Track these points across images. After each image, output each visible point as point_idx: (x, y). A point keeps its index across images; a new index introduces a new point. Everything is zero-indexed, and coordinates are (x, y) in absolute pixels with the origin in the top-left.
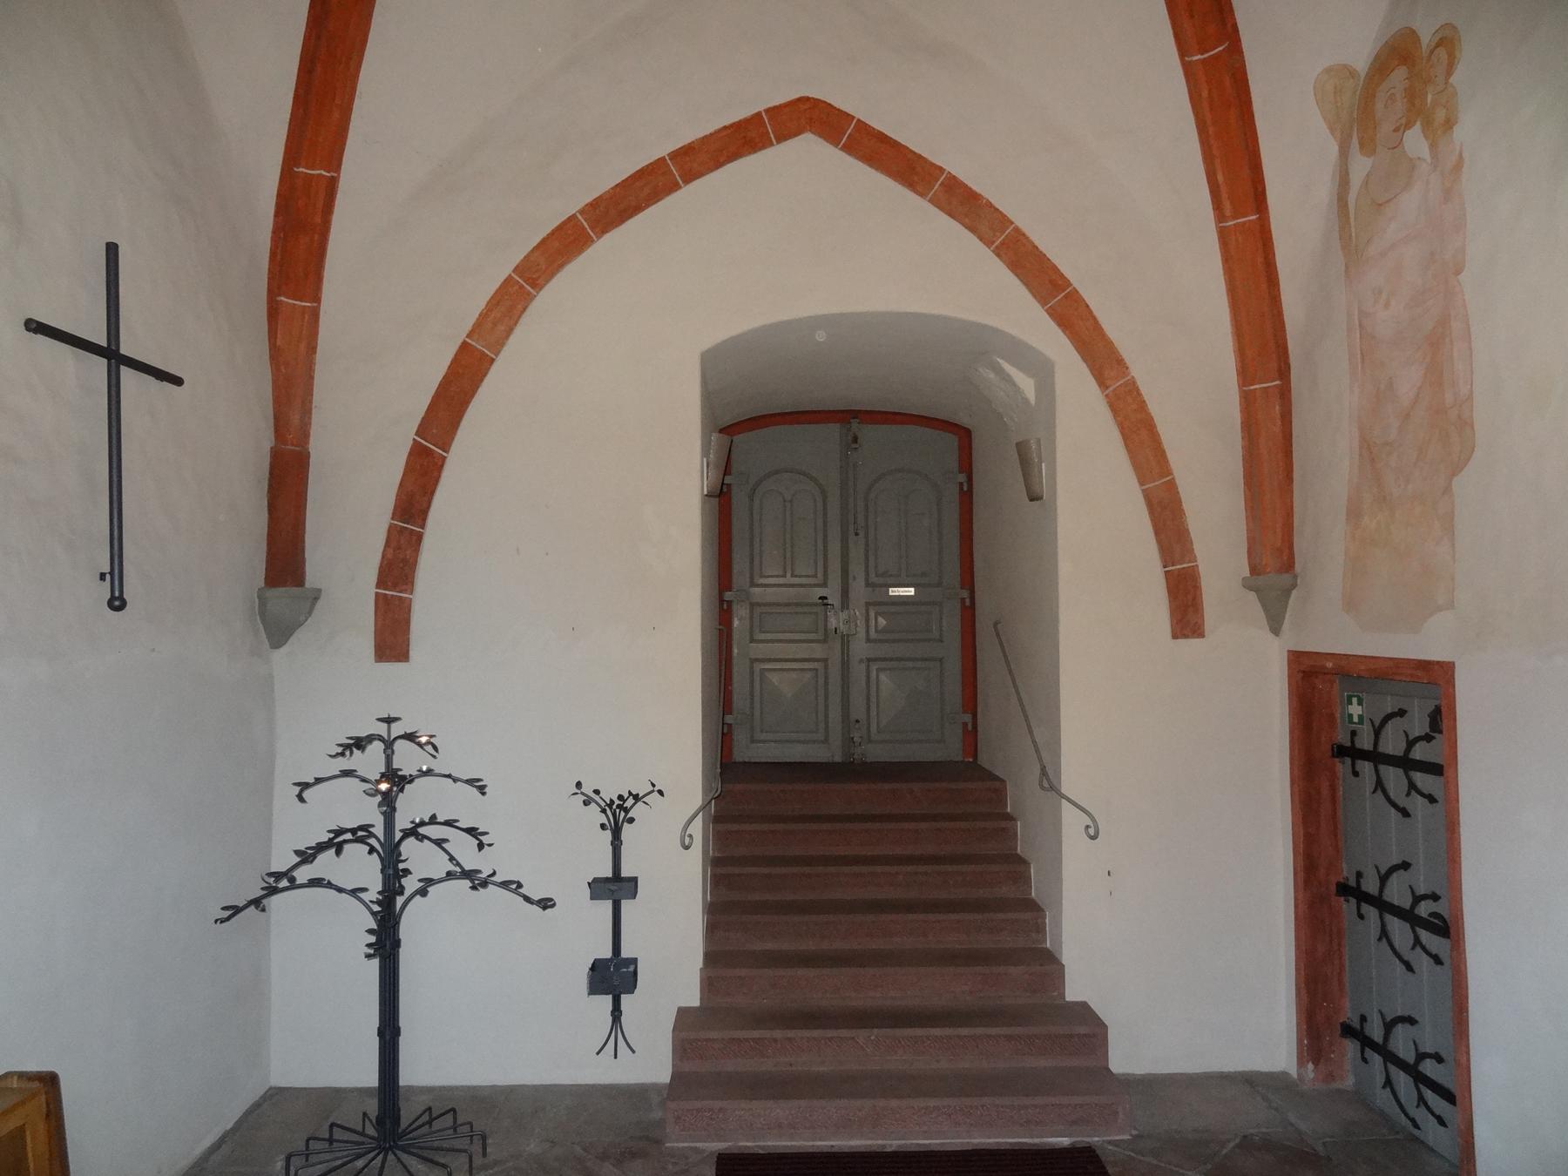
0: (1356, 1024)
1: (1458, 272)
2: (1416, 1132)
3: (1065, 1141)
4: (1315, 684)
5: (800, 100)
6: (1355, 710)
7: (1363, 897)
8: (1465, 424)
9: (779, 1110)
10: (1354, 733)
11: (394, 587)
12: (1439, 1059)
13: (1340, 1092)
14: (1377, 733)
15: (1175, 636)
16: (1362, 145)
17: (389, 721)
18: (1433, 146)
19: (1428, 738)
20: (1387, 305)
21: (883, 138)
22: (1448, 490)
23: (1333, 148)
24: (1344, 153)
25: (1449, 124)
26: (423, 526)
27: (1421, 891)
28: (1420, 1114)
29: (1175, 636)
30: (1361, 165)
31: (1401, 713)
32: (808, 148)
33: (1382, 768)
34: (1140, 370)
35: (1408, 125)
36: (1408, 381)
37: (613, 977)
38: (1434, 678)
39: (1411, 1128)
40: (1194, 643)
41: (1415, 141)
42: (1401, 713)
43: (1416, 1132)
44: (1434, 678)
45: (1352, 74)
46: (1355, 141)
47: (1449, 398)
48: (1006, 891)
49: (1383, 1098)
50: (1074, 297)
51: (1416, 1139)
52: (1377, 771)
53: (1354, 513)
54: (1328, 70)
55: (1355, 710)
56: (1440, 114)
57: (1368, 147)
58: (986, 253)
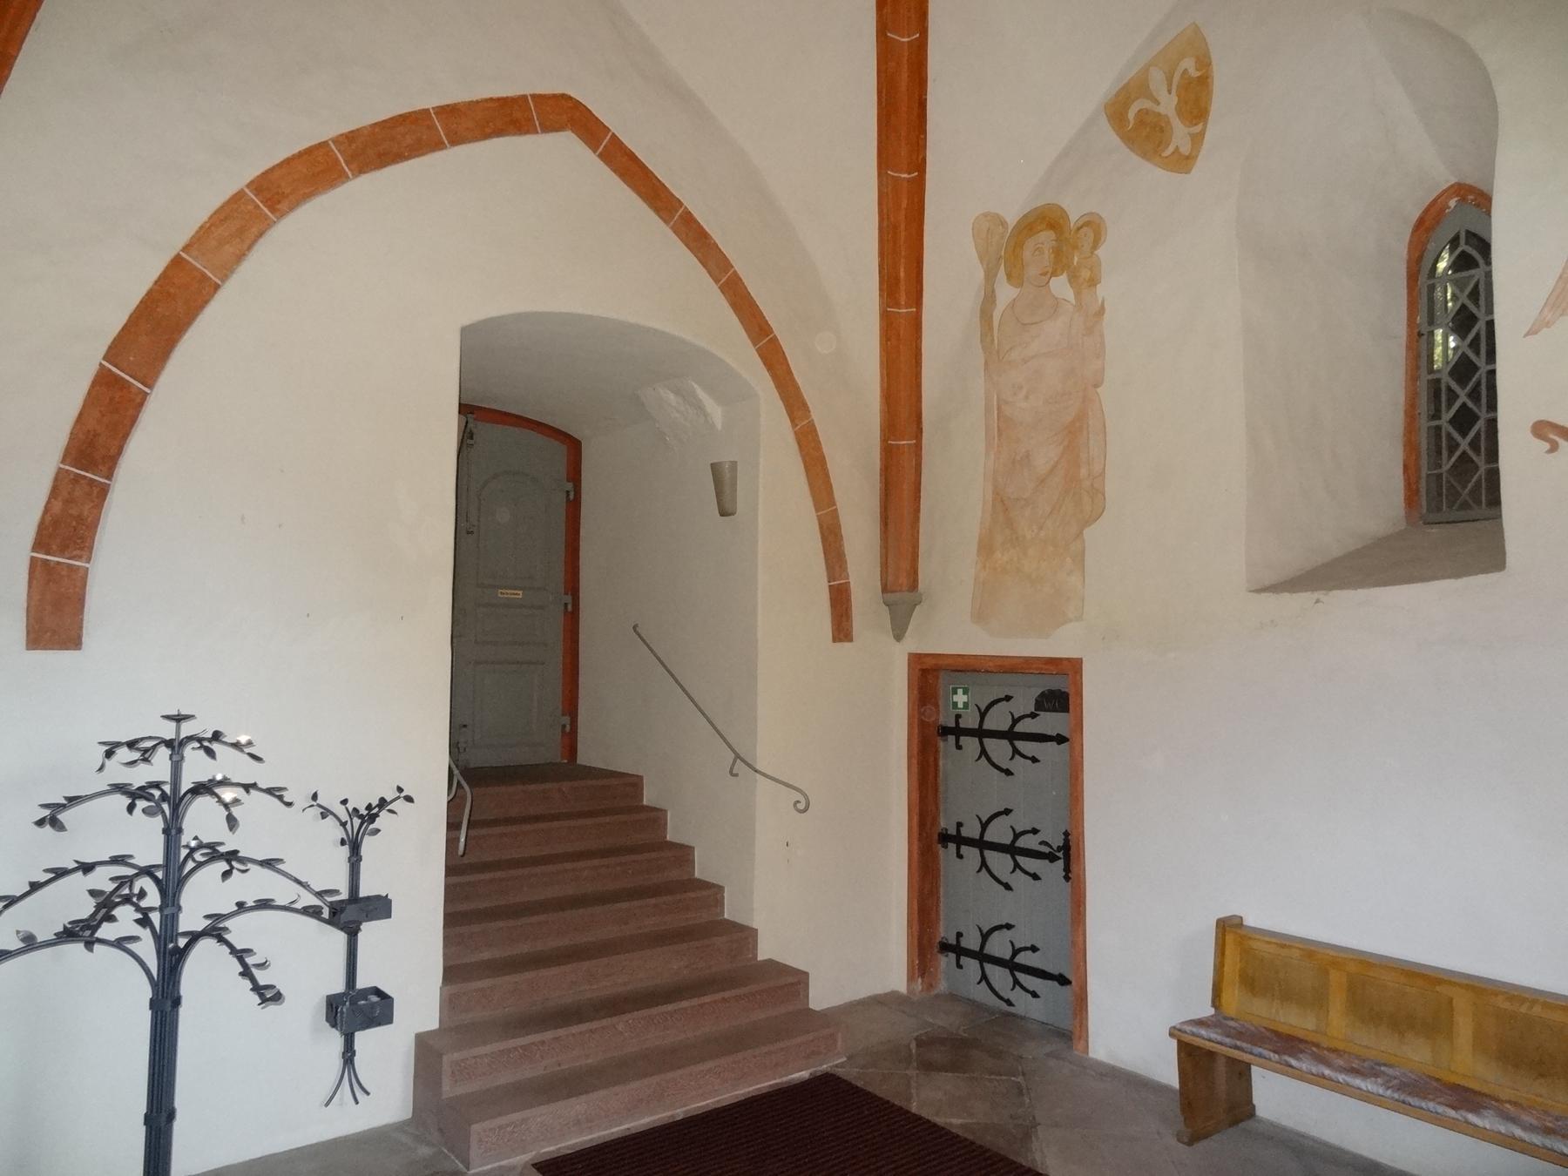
0: (952, 941)
1: (1096, 386)
2: (1011, 1009)
3: (804, 1075)
4: (929, 677)
5: (563, 96)
6: (960, 698)
7: (960, 840)
8: (1097, 493)
9: (577, 1106)
10: (958, 717)
11: (62, 551)
12: (1034, 949)
13: (937, 996)
14: (983, 715)
15: (834, 640)
16: (1009, 276)
17: (179, 719)
18: (1078, 294)
19: (1033, 716)
20: (1027, 397)
21: (632, 157)
22: (1080, 534)
24: (990, 277)
25: (1093, 282)
26: (109, 476)
27: (1019, 829)
28: (1017, 996)
29: (834, 640)
30: (1006, 293)
31: (1008, 698)
32: (565, 145)
34: (818, 415)
35: (1054, 274)
36: (1045, 456)
37: (357, 1009)
38: (1072, 667)
39: (1004, 1006)
40: (847, 644)
41: (1060, 286)
42: (1008, 698)
43: (1011, 1009)
44: (1072, 667)
45: (1003, 223)
46: (1002, 273)
47: (1083, 472)
48: (674, 874)
49: (981, 994)
51: (1014, 1015)
52: (981, 743)
53: (986, 548)
54: (985, 215)
55: (960, 698)
56: (1085, 274)
57: (1015, 277)
58: (715, 288)
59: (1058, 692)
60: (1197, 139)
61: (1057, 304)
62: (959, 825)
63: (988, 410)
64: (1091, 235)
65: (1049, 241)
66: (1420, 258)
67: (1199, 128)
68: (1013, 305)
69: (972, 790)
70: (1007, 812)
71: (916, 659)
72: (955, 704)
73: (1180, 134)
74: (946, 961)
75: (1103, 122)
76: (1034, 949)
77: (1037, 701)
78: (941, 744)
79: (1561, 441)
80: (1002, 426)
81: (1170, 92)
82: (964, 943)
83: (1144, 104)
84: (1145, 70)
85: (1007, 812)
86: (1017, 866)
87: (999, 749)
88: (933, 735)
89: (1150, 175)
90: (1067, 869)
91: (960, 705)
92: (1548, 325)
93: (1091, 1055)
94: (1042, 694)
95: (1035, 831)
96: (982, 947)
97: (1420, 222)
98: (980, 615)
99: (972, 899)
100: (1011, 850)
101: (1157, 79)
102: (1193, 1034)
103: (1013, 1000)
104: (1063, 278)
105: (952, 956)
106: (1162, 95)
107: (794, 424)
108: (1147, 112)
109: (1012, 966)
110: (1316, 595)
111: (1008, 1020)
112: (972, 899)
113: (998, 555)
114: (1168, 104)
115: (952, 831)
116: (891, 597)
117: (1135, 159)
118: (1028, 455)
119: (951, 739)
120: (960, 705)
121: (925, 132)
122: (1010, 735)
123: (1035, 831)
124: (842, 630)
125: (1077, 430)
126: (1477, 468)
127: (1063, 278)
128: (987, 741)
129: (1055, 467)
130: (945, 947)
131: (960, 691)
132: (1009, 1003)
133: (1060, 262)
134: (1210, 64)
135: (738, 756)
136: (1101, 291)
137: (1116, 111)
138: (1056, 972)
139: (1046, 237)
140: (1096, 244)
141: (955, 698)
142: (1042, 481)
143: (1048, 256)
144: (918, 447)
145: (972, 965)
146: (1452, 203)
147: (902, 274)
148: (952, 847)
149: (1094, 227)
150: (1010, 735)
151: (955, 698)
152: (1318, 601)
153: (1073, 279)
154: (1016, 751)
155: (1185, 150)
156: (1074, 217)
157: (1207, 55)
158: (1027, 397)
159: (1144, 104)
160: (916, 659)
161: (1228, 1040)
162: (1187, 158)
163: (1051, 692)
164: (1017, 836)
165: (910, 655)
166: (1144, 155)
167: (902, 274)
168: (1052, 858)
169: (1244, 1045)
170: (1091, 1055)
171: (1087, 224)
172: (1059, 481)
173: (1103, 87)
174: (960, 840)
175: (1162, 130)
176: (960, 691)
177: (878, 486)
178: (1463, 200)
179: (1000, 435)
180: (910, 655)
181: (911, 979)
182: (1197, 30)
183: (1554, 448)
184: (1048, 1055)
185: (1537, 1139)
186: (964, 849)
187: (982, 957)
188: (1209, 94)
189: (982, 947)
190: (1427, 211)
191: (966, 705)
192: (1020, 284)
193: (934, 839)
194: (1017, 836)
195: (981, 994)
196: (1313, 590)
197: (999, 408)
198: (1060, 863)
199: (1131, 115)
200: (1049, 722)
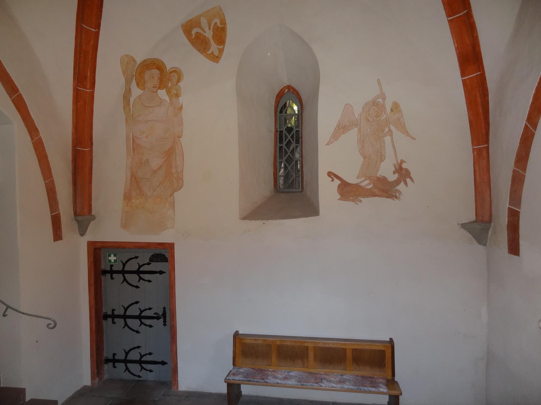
0: (111, 357)
1: (179, 137)
4: (97, 251)
6: (112, 258)
8: (180, 179)
10: (112, 266)
12: (150, 354)
14: (124, 265)
16: (138, 85)
18: (170, 99)
19: (148, 264)
20: (147, 137)
22: (172, 195)
23: (123, 80)
24: (128, 82)
25: (177, 95)
28: (143, 374)
30: (136, 91)
31: (136, 257)
33: (126, 275)
35: (159, 88)
36: (156, 162)
38: (171, 246)
39: (136, 378)
40: (60, 242)
41: (162, 94)
42: (136, 257)
44: (171, 246)
45: (134, 61)
46: (134, 81)
47: (174, 170)
50: (20, 97)
51: (143, 381)
52: (124, 277)
53: (127, 197)
54: (127, 56)
55: (112, 258)
56: (174, 92)
59: (162, 255)
60: (221, 51)
61: (161, 101)
62: (113, 310)
63: (127, 139)
64: (176, 75)
65: (154, 74)
66: (277, 106)
67: (221, 47)
68: (140, 97)
69: (118, 295)
71: (91, 244)
72: (110, 261)
73: (214, 48)
74: (108, 367)
75: (181, 31)
76: (150, 354)
77: (150, 258)
78: (103, 278)
79: (335, 178)
80: (134, 146)
81: (210, 29)
82: (117, 357)
83: (199, 30)
84: (199, 17)
85: (137, 302)
86: (142, 323)
89: (201, 58)
90: (165, 321)
91: (113, 261)
92: (332, 143)
93: (180, 389)
94: (153, 256)
95: (150, 309)
96: (126, 357)
97: (278, 94)
98: (125, 225)
99: (119, 338)
101: (204, 22)
102: (233, 380)
103: (140, 375)
104: (164, 91)
105: (111, 364)
106: (207, 29)
107: (32, 139)
108: (200, 34)
109: (140, 362)
110: (264, 221)
111: (140, 383)
112: (119, 338)
113: (134, 200)
114: (209, 34)
115: (110, 313)
116: (79, 218)
117: (195, 51)
118: (148, 160)
119: (108, 275)
120: (113, 261)
121: (101, 11)
122: (138, 272)
123: (150, 309)
124: (57, 235)
125: (171, 153)
126: (292, 176)
127: (164, 91)
128: (126, 275)
129: (160, 168)
130: (107, 361)
131: (112, 255)
132: (139, 376)
133: (162, 84)
134: (226, 24)
135: (8, 307)
136: (182, 100)
137: (187, 28)
138: (160, 360)
139: (156, 72)
140: (179, 80)
141: (110, 258)
142: (155, 172)
143: (156, 81)
144: (91, 151)
145: (121, 366)
146: (286, 91)
147: (89, 74)
148: (110, 320)
149: (177, 73)
150: (138, 272)
151: (110, 258)
152: (264, 223)
153: (168, 92)
154: (140, 278)
155: (216, 53)
156: (169, 66)
157: (225, 20)
158: (147, 137)
159: (199, 30)
160: (91, 244)
161: (246, 379)
162: (217, 57)
163: (157, 255)
166: (199, 51)
167: (89, 74)
168: (158, 318)
169: (251, 379)
170: (180, 389)
171: (175, 71)
172: (160, 172)
173: (183, 17)
174: (113, 316)
175: (206, 43)
176: (112, 255)
177: (71, 166)
178: (289, 90)
179: (134, 151)
181: (93, 378)
182: (220, 9)
183: (333, 180)
184: (164, 395)
185: (339, 386)
186: (116, 320)
187: (126, 361)
188: (225, 35)
190: (280, 91)
191: (115, 261)
192: (144, 89)
193: (101, 317)
194: (142, 312)
195: (127, 376)
196: (262, 219)
197: (133, 140)
198: (162, 320)
199: (194, 32)
200: (156, 266)
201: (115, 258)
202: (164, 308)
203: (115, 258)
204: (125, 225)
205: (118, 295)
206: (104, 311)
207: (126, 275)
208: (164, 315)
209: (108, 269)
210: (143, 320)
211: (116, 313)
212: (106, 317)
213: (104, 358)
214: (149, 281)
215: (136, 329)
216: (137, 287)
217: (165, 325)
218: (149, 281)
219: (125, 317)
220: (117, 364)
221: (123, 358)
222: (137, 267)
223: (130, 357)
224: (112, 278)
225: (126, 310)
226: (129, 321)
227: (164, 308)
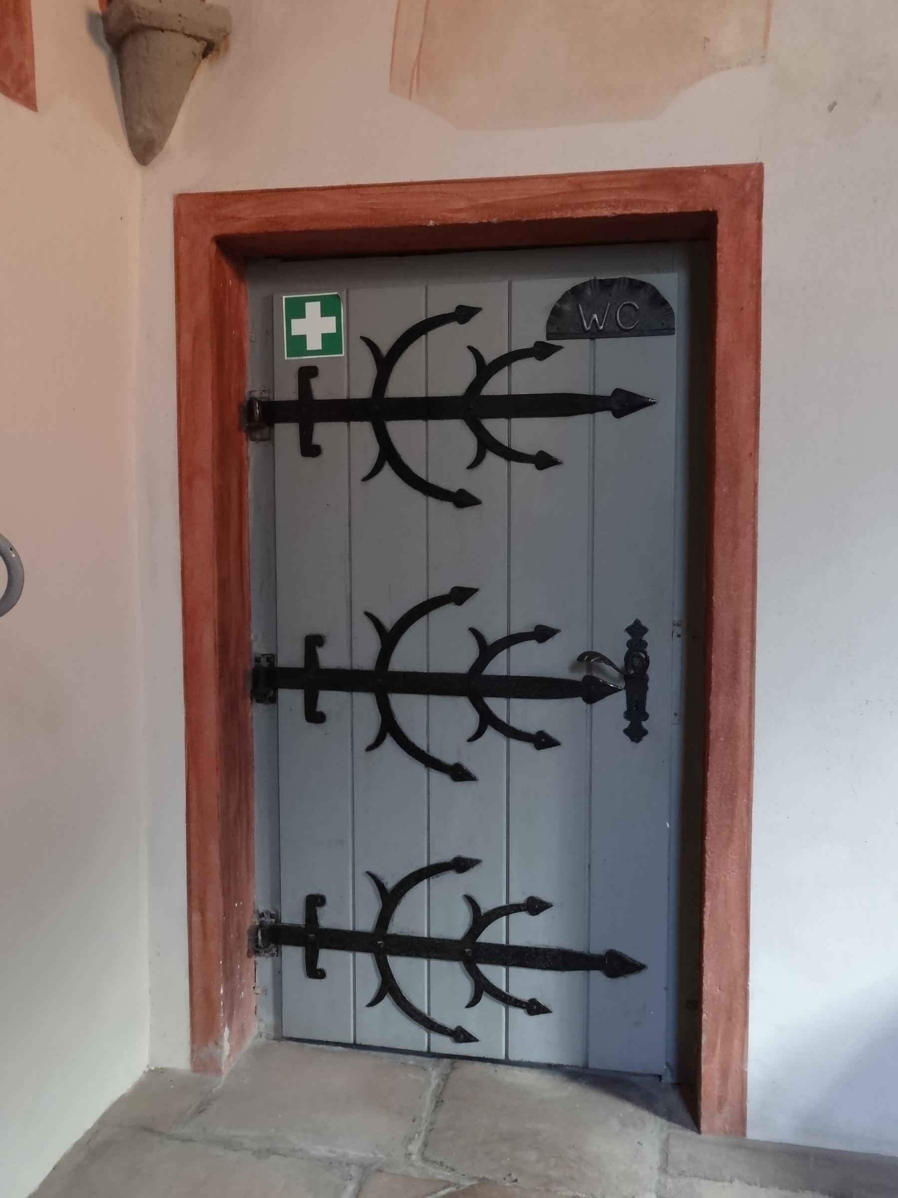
6: (314, 326)
7: (313, 679)
10: (307, 374)
19: (541, 351)
27: (492, 635)
28: (487, 1022)
31: (464, 314)
39: (444, 1044)
62: (314, 642)
69: (353, 546)
70: (460, 595)
71: (191, 209)
77: (556, 312)
82: (327, 919)
85: (460, 595)
86: (487, 720)
87: (436, 447)
88: (243, 419)
91: (314, 343)
95: (542, 634)
96: (384, 918)
100: (474, 686)
115: (291, 656)
120: (314, 343)
122: (471, 407)
123: (542, 634)
128: (395, 428)
132: (461, 1035)
141: (298, 327)
145: (352, 971)
150: (471, 407)
151: (298, 327)
160: (191, 209)
164: (487, 651)
165: (180, 199)
168: (591, 691)
174: (313, 679)
180: (180, 199)
186: (327, 700)
187: (382, 943)
189: (384, 918)
191: (330, 342)
194: (487, 651)
198: (618, 702)
201: (329, 325)
202: (637, 631)
203: (329, 325)
204: (420, 72)
205: (353, 546)
206: (258, 648)
207: (395, 428)
208: (636, 677)
209: (287, 391)
210: (497, 705)
211: (328, 658)
212: (267, 680)
213: (251, 921)
214: (544, 461)
215: (449, 759)
216: (463, 500)
217: (636, 733)
218: (544, 461)
219: (382, 682)
220: (327, 958)
221: (366, 923)
222: (468, 372)
223: (409, 919)
224: (310, 449)
225: (389, 639)
226: (408, 708)
227: (637, 631)
